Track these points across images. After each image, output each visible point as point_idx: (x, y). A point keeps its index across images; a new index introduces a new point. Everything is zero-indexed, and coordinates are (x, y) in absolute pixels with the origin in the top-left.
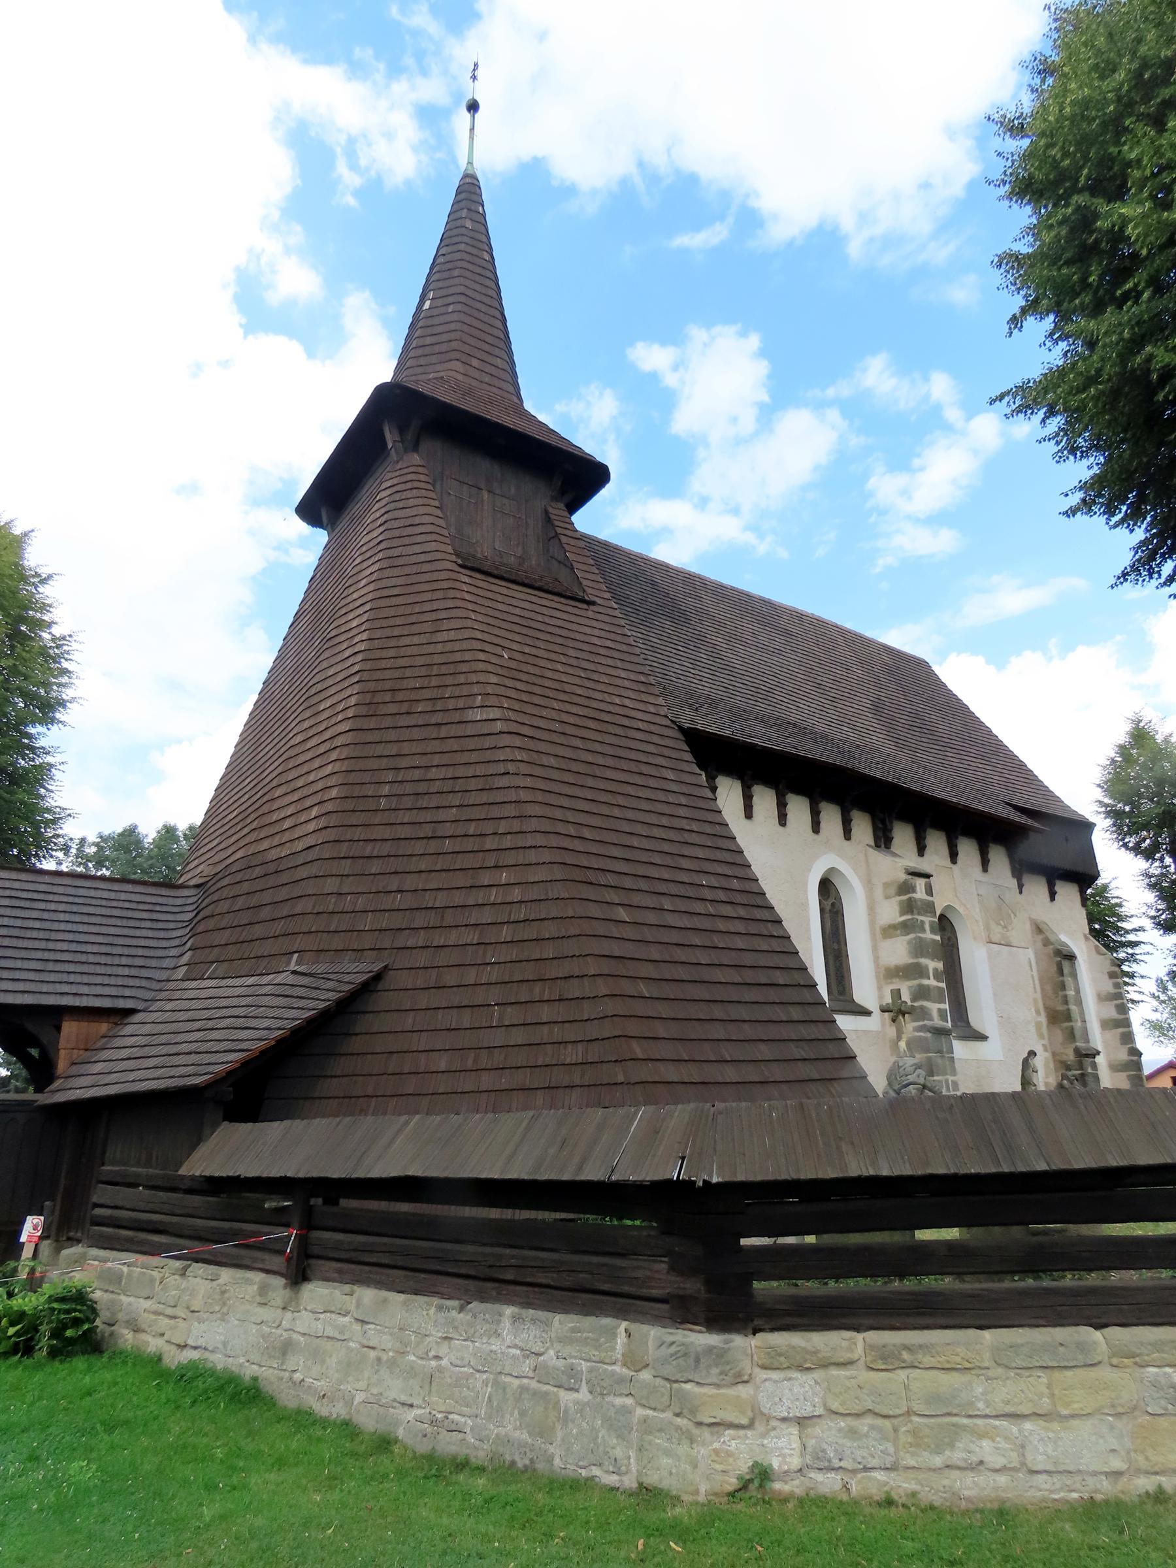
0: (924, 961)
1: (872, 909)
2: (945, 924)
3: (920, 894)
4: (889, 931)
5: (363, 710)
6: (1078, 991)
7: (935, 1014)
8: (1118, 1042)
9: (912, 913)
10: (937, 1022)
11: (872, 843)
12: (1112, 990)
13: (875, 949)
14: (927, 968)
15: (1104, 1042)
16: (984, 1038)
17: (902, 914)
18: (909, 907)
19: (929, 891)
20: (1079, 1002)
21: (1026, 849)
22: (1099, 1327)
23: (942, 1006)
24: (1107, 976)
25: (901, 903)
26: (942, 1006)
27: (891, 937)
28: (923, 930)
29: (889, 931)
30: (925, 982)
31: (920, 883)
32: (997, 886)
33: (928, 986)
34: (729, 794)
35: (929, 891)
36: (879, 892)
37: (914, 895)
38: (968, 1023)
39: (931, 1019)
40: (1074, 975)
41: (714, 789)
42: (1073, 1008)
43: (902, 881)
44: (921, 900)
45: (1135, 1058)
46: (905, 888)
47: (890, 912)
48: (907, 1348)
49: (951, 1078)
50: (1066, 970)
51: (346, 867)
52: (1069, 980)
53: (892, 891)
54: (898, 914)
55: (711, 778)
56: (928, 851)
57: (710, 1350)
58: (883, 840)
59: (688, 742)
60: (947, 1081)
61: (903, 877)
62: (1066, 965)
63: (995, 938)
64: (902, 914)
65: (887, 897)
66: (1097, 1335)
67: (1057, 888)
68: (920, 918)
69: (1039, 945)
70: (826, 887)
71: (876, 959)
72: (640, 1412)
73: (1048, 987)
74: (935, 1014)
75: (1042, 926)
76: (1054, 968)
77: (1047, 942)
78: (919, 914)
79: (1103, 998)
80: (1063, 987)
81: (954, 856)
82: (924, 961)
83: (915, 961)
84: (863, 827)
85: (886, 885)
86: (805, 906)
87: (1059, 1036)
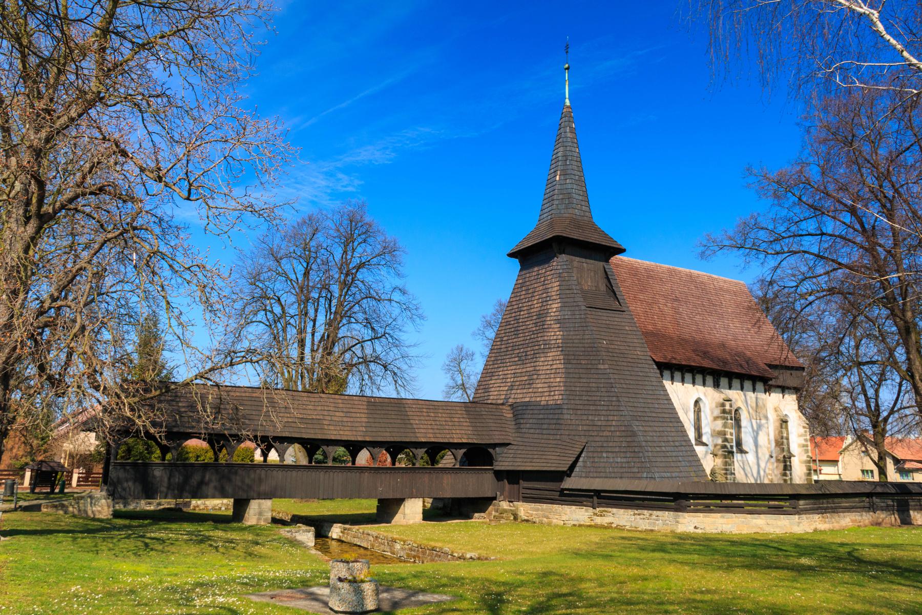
0: (727, 430)
7: (729, 447)
16: (746, 452)
19: (731, 406)
21: (770, 383)
31: (727, 404)
34: (667, 373)
40: (787, 428)
42: (785, 441)
46: (723, 405)
47: (717, 412)
50: (784, 426)
52: (784, 430)
59: (657, 366)
61: (722, 401)
62: (784, 425)
70: (697, 402)
73: (777, 432)
77: (778, 416)
84: (710, 380)
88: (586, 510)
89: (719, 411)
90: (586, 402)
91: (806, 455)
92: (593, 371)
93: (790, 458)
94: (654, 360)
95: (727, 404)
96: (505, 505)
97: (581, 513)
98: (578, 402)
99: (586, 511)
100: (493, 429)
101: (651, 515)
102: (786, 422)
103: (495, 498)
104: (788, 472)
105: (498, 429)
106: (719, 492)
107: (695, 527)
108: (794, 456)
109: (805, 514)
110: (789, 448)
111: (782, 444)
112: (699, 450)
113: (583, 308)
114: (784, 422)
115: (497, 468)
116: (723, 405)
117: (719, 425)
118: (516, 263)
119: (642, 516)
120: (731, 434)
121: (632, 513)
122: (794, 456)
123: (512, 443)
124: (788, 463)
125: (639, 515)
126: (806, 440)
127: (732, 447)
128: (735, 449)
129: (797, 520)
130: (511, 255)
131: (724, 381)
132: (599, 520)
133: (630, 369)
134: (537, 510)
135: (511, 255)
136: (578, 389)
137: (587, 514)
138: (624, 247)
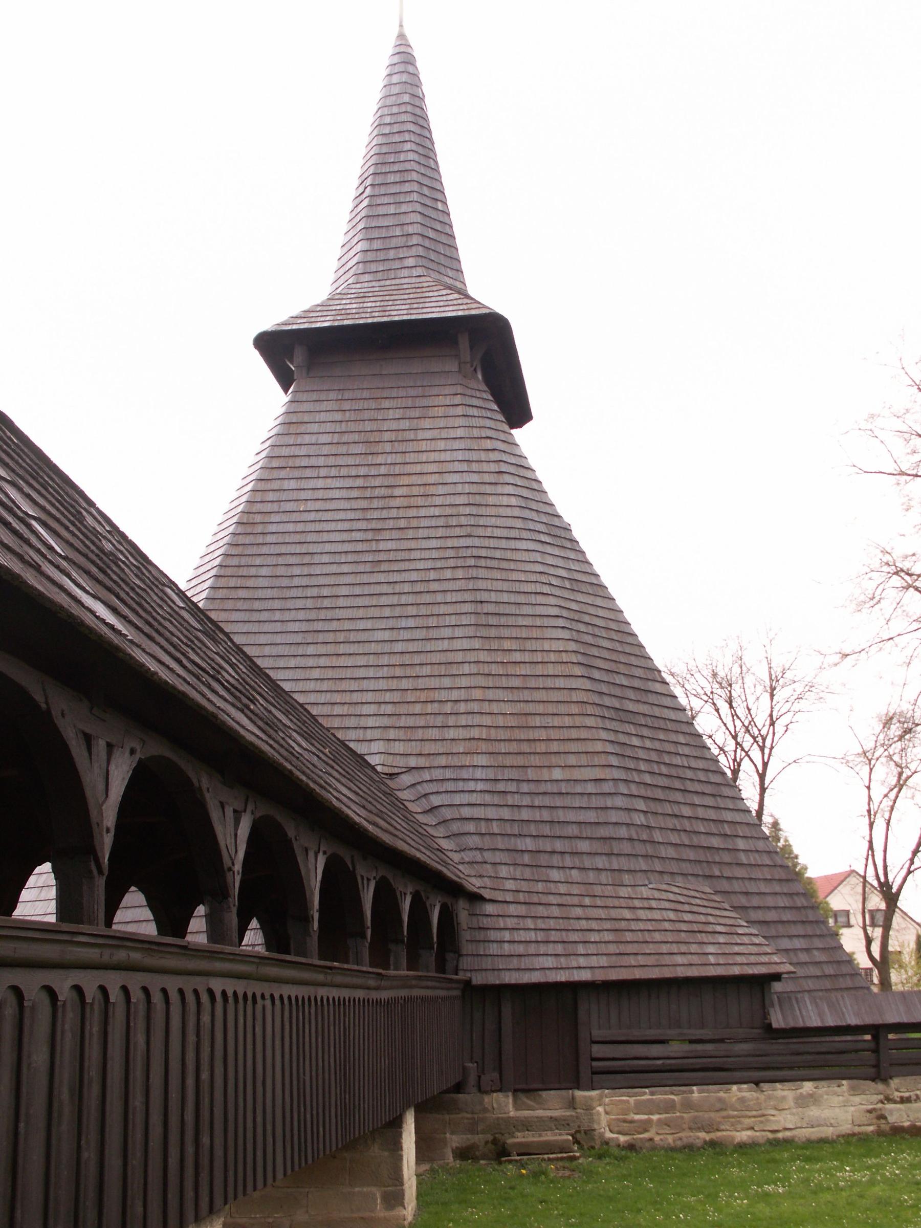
97: (836, 1100)
99: (854, 1091)
123: (486, 894)
134: (669, 1107)
137: (857, 1099)
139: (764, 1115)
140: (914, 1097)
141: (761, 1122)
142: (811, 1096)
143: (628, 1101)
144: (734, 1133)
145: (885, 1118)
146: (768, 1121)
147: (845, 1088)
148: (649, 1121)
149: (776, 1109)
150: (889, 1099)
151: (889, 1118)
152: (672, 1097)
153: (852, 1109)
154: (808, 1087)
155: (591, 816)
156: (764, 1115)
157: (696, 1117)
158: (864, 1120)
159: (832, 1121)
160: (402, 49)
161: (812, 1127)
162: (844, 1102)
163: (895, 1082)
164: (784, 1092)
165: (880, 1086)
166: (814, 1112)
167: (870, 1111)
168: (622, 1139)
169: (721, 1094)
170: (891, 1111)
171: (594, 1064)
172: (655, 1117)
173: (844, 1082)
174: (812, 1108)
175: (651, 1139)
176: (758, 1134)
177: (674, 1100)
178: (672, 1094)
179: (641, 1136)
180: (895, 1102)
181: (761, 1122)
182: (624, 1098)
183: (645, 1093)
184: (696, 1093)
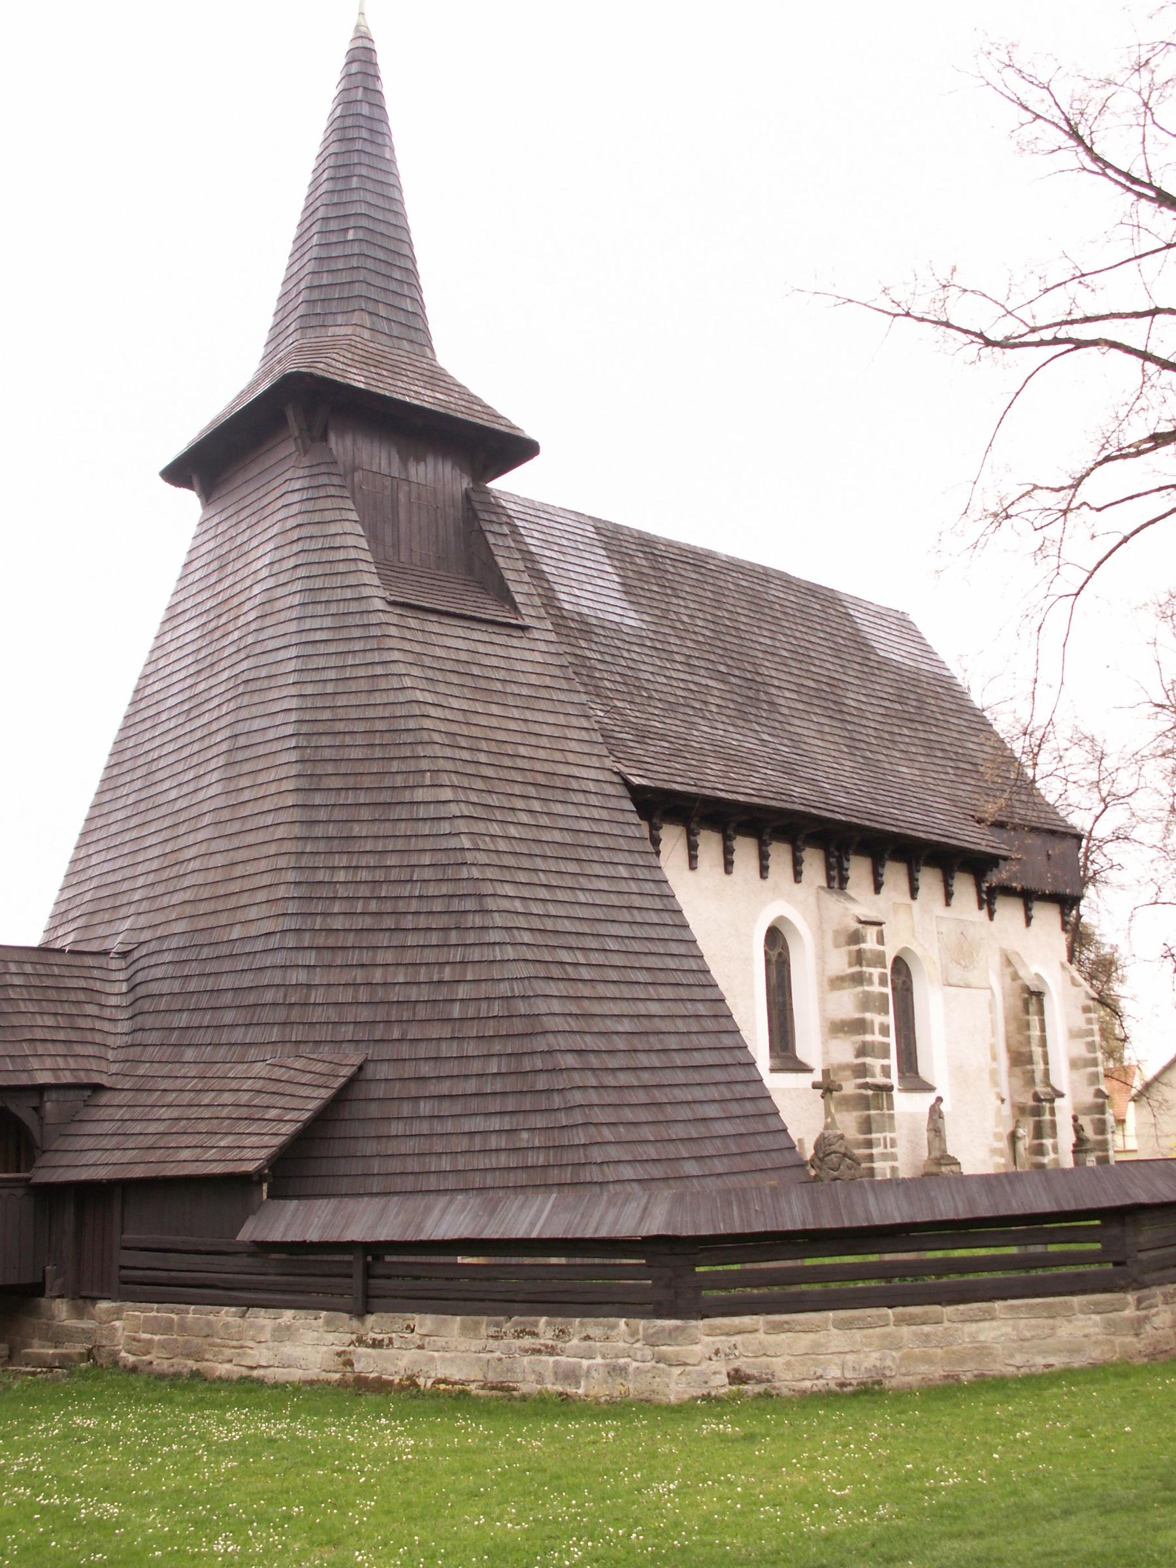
0: (868, 1016)
1: (821, 957)
2: (901, 968)
3: (870, 944)
4: (837, 982)
5: (303, 783)
6: (1043, 1029)
7: (878, 1070)
8: (1085, 1082)
9: (861, 965)
10: (880, 1080)
11: (825, 884)
12: (1085, 1027)
13: (822, 1001)
14: (872, 1022)
15: (1072, 1082)
17: (850, 965)
18: (859, 958)
19: (881, 940)
20: (1043, 1042)
21: (995, 878)
22: (890, 1307)
23: (885, 1062)
24: (1080, 1011)
25: (850, 952)
26: (885, 1062)
27: (839, 989)
28: (870, 982)
29: (837, 982)
30: (868, 1038)
32: (961, 921)
33: (873, 1042)
34: (672, 840)
35: (881, 940)
36: (829, 938)
37: (863, 946)
38: (917, 1073)
39: (873, 1076)
40: (1041, 1012)
41: (656, 841)
42: (1037, 1051)
43: (853, 929)
44: (872, 951)
45: (1100, 1100)
46: (855, 938)
47: (839, 963)
48: (787, 1322)
49: (889, 1135)
51: (311, 958)
52: (1034, 1020)
53: (843, 939)
54: (846, 965)
55: (654, 828)
56: (884, 889)
57: (677, 1328)
58: (837, 880)
59: (634, 801)
60: (885, 1139)
63: (952, 981)
64: (850, 965)
65: (837, 946)
66: (890, 1311)
67: (1034, 912)
68: (872, 970)
69: (1008, 980)
70: (775, 937)
71: (823, 1010)
72: (635, 1364)
74: (878, 1070)
75: (1014, 960)
76: (1020, 1004)
78: (869, 966)
79: (1075, 1035)
80: (1028, 1026)
81: (914, 891)
82: (868, 1016)
83: (860, 1016)
84: (814, 864)
85: (837, 933)
86: (748, 960)
87: (1018, 1083)
88: (328, 1322)
89: (846, 960)
90: (368, 922)
91: (1092, 1089)
92: (397, 812)
93: (1052, 1101)
94: (627, 783)
95: (871, 933)
96: (61, 1311)
97: (310, 1336)
98: (337, 924)
100: (39, 1034)
101: (562, 1333)
102: (1039, 995)
103: (37, 1290)
104: (1048, 1142)
105: (61, 1036)
106: (828, 1223)
107: (737, 1377)
108: (1061, 1095)
109: (1160, 1283)
110: (1046, 1073)
111: (1030, 1060)
112: (781, 1086)
113: (379, 604)
114: (1032, 993)
115: (43, 1176)
116: (855, 938)
117: (845, 1005)
118: (188, 501)
119: (528, 1342)
120: (884, 1031)
121: (492, 1330)
122: (1061, 1095)
124: (1047, 1117)
125: (519, 1335)
126: (1091, 1046)
127: (886, 1071)
128: (894, 1080)
129: (1130, 1312)
130: (177, 473)
131: (859, 869)
132: (368, 1363)
133: (536, 806)
134: (168, 1327)
135: (177, 473)
136: (341, 876)
137: (331, 1337)
138: (530, 432)
139: (242, 1347)
140: (386, 1341)
141: (239, 1355)
142: (288, 1328)
143: (138, 1317)
144: (217, 1365)
145: (352, 1365)
146: (245, 1354)
147: (321, 1321)
148: (150, 1341)
149: (253, 1339)
150: (361, 1341)
151: (355, 1365)
152: (173, 1316)
153: (325, 1349)
154: (288, 1315)
155: (247, 980)
156: (242, 1347)
157: (187, 1342)
158: (331, 1365)
159: (303, 1362)
160: (359, 43)
161: (283, 1367)
162: (318, 1339)
163: (371, 1319)
164: (264, 1320)
165: (355, 1323)
166: (289, 1349)
167: (339, 1354)
168: (132, 1358)
169: (211, 1317)
170: (360, 1356)
171: (124, 1272)
172: (156, 1338)
173: (324, 1314)
174: (287, 1343)
175: (151, 1363)
176: (236, 1368)
177: (173, 1320)
178: (172, 1312)
179: (144, 1358)
180: (368, 1346)
181: (239, 1355)
182: (137, 1313)
183: (152, 1310)
184: (192, 1314)
